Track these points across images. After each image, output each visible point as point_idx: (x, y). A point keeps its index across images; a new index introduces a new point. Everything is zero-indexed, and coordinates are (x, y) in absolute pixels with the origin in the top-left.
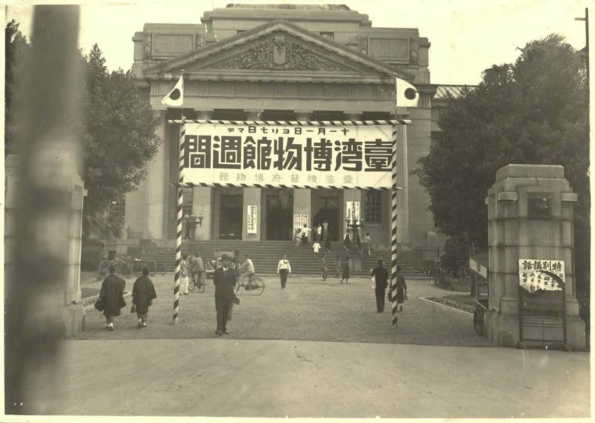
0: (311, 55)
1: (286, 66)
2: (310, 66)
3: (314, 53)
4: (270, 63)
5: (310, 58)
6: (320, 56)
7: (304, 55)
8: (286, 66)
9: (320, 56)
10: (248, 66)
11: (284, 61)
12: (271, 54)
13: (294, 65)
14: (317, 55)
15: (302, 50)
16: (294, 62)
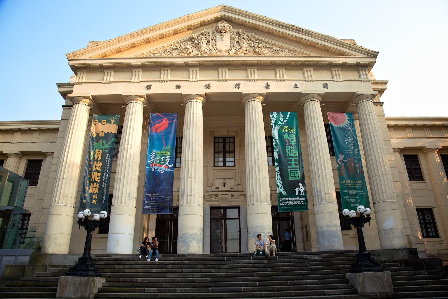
0: (257, 41)
1: (230, 51)
2: (257, 50)
3: (260, 40)
4: (213, 50)
5: (256, 44)
6: (267, 43)
7: (250, 42)
8: (232, 53)
9: (267, 43)
10: (188, 52)
11: (228, 48)
12: (214, 42)
13: (240, 50)
14: (264, 41)
15: (247, 37)
16: (239, 48)
